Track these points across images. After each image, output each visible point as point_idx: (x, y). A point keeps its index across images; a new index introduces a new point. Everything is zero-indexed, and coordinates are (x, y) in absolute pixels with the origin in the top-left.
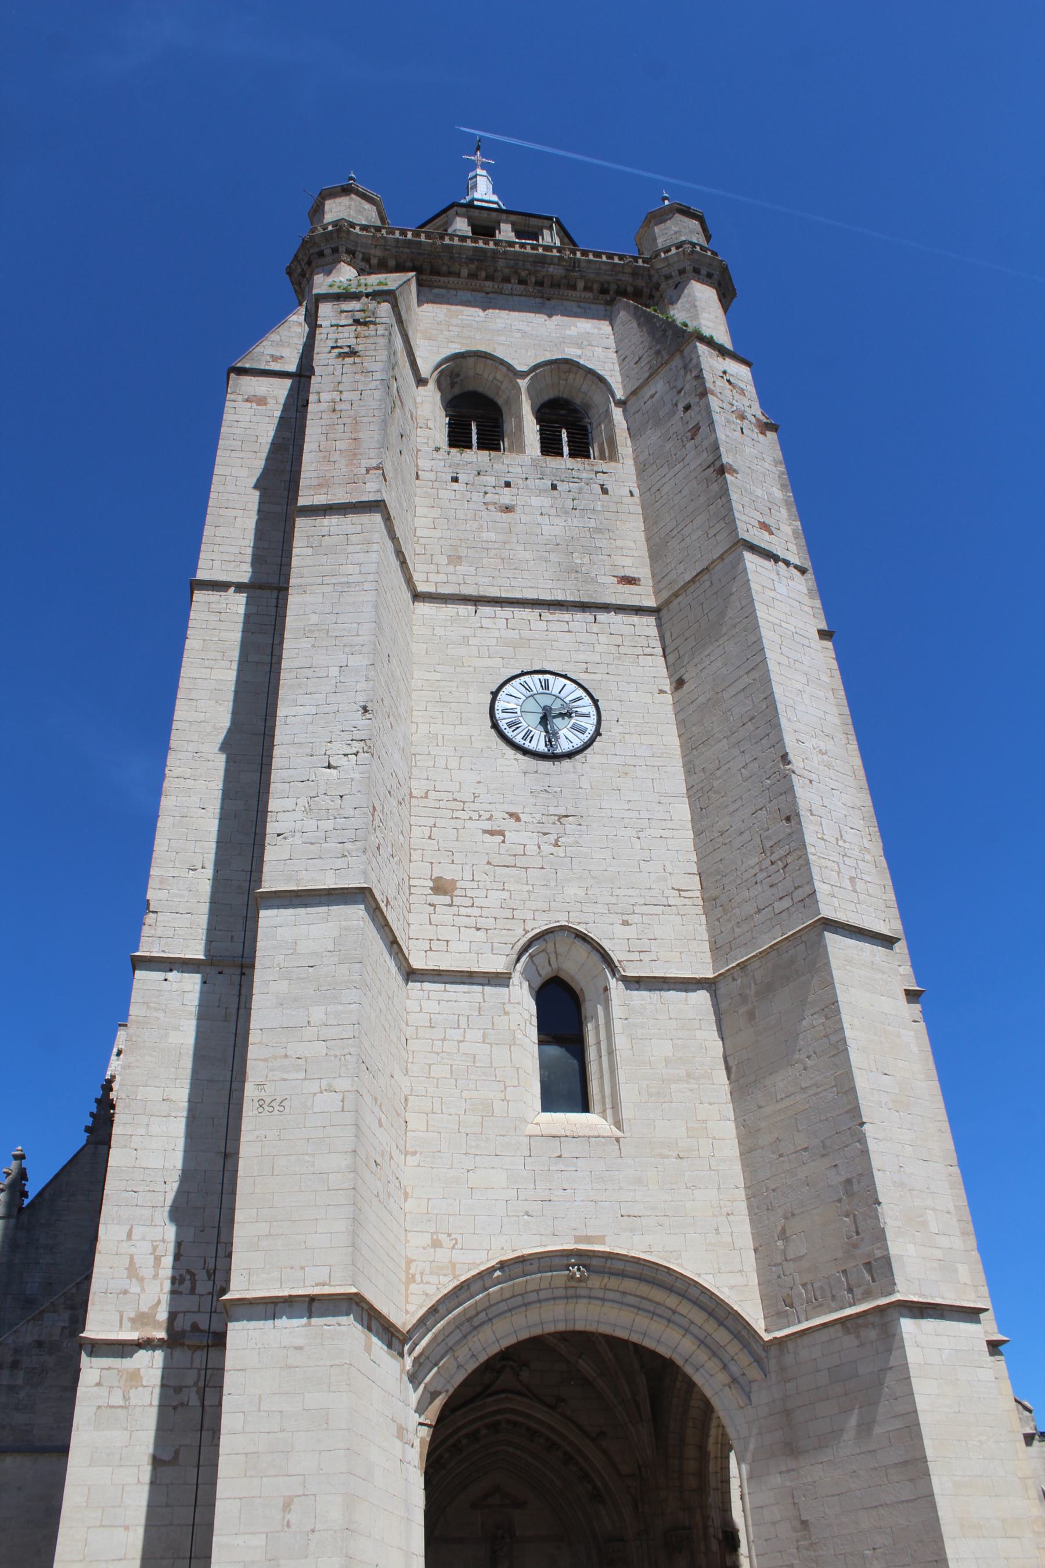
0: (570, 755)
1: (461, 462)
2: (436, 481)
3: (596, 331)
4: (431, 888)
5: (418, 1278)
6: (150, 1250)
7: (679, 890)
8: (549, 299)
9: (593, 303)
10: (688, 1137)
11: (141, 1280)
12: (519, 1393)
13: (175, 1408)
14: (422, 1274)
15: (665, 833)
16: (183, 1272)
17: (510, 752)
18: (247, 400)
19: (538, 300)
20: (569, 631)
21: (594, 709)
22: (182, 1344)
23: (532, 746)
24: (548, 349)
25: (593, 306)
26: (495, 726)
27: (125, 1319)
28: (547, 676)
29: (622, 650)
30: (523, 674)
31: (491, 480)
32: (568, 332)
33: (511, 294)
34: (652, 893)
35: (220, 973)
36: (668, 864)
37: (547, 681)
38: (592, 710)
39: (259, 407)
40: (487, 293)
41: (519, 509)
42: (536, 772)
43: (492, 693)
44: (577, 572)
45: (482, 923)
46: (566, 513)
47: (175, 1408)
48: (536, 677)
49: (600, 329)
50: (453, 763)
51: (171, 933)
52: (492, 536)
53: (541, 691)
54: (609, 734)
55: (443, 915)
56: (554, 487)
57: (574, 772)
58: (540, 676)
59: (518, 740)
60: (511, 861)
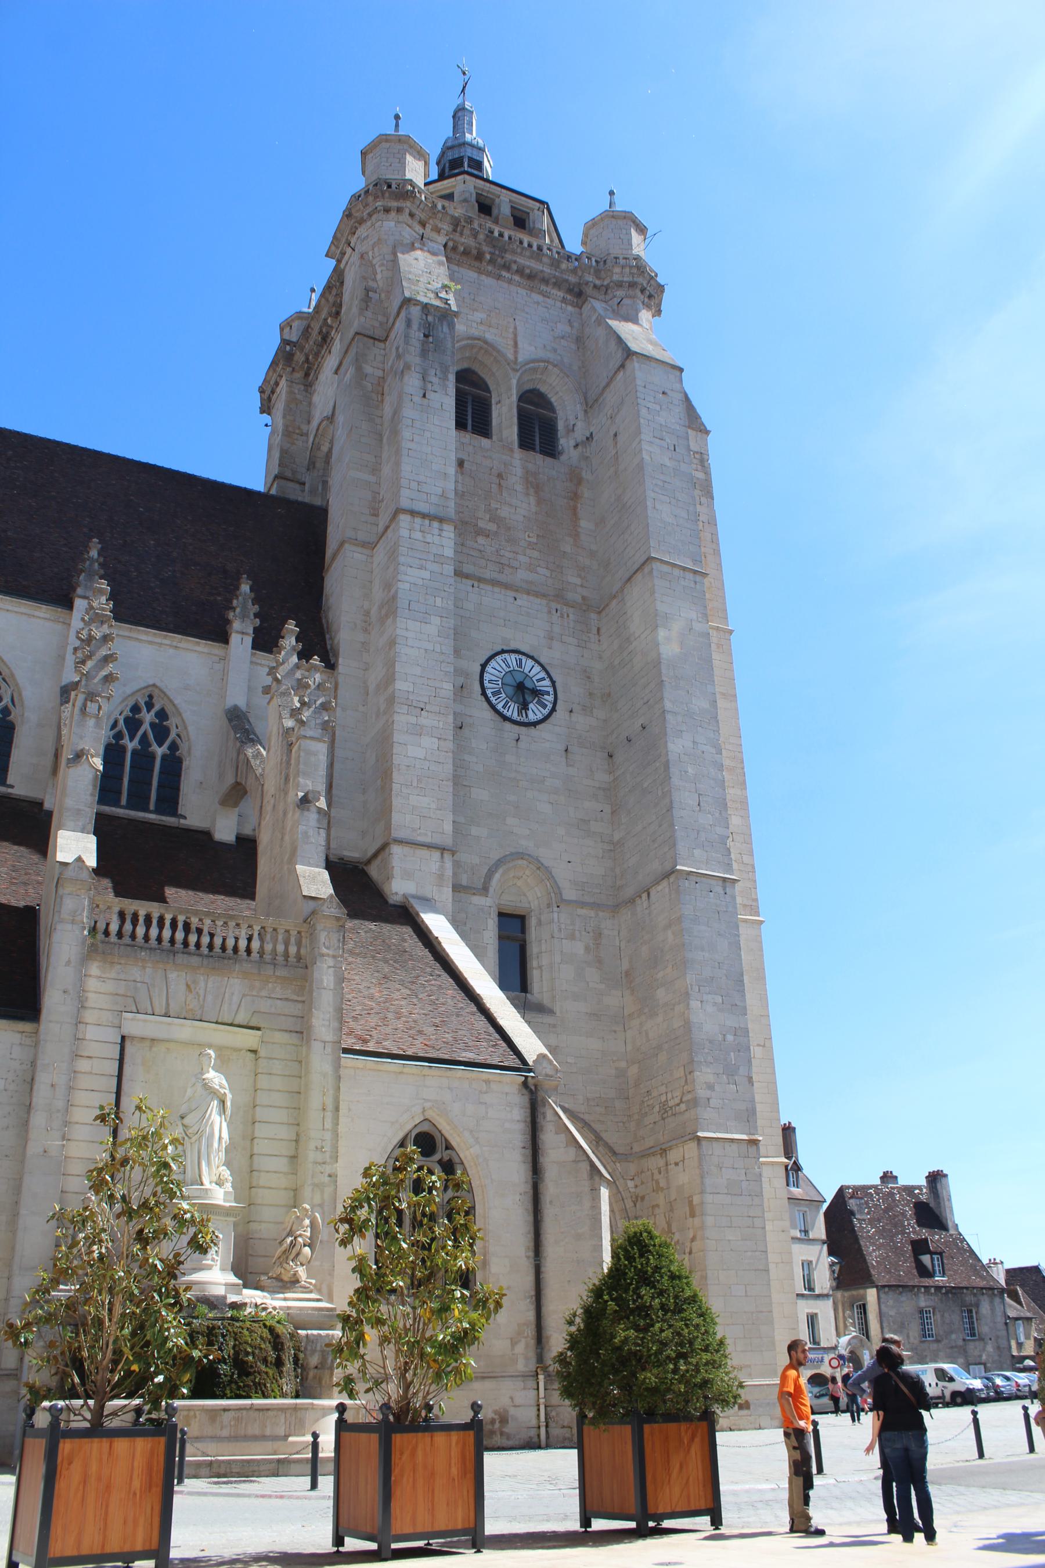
0: (535, 724)
23: (509, 714)
26: (484, 693)
30: (503, 652)
37: (521, 660)
38: (551, 690)
53: (516, 668)
59: (499, 707)
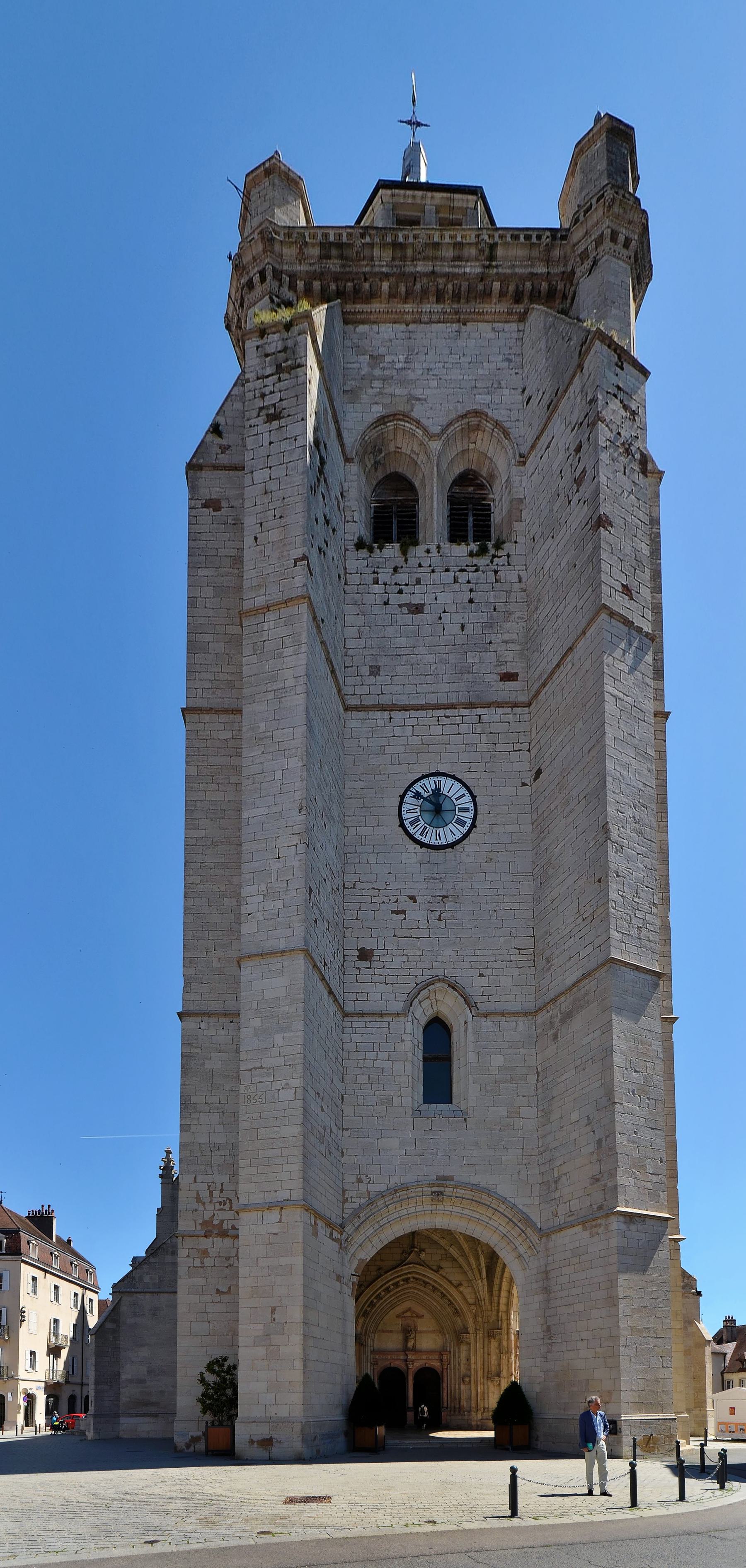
1: (381, 560)
2: (360, 584)
3: (506, 364)
4: (358, 957)
5: (349, 1199)
6: (207, 1188)
7: (519, 949)
8: (465, 324)
9: (506, 322)
10: (508, 1117)
11: (204, 1204)
13: (227, 1267)
14: (351, 1197)
15: (516, 906)
16: (225, 1199)
17: (412, 847)
18: (205, 506)
19: (455, 326)
20: (459, 734)
21: (472, 805)
22: (228, 1236)
24: (461, 400)
25: (507, 326)
26: (402, 825)
27: (197, 1225)
28: (439, 778)
29: (499, 747)
30: (423, 777)
31: (402, 578)
32: (480, 372)
33: (431, 322)
34: (502, 952)
35: (231, 1022)
36: (514, 930)
38: (471, 806)
39: (215, 513)
40: (407, 325)
41: (426, 609)
42: (429, 862)
43: (400, 796)
44: (469, 673)
45: (389, 979)
46: (464, 608)
47: (227, 1267)
48: (432, 779)
49: (510, 361)
50: (372, 860)
51: (199, 997)
52: (403, 641)
54: (482, 826)
55: (365, 976)
56: (456, 580)
57: (455, 860)
58: (436, 779)
59: (417, 836)
60: (408, 933)
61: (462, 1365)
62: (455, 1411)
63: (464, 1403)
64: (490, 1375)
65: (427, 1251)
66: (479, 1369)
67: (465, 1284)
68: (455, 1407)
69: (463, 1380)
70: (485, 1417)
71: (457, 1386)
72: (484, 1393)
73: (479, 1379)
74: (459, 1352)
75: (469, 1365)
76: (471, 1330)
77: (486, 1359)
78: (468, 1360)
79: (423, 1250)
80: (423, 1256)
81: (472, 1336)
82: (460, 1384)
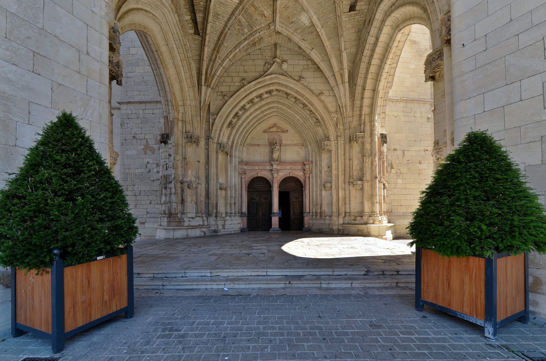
12: (282, 74)
61: (323, 172)
62: (316, 216)
63: (325, 208)
64: (351, 180)
65: (290, 62)
66: (340, 175)
67: (327, 93)
68: (316, 213)
69: (324, 186)
70: (346, 222)
71: (319, 192)
72: (345, 198)
73: (340, 184)
74: (321, 161)
75: (331, 171)
76: (332, 138)
77: (348, 165)
78: (329, 167)
79: (286, 61)
80: (285, 66)
81: (333, 144)
82: (321, 190)
